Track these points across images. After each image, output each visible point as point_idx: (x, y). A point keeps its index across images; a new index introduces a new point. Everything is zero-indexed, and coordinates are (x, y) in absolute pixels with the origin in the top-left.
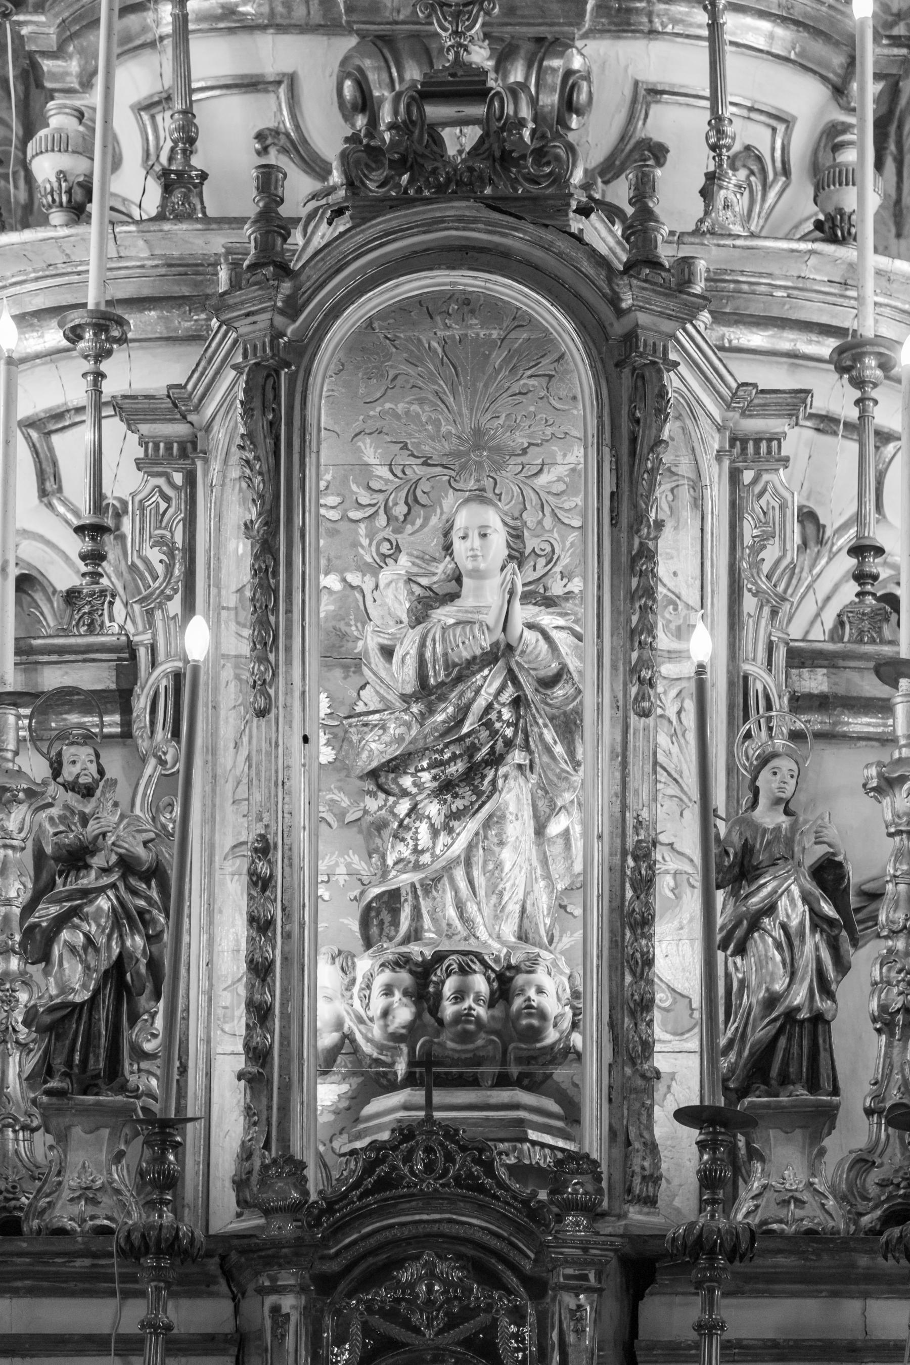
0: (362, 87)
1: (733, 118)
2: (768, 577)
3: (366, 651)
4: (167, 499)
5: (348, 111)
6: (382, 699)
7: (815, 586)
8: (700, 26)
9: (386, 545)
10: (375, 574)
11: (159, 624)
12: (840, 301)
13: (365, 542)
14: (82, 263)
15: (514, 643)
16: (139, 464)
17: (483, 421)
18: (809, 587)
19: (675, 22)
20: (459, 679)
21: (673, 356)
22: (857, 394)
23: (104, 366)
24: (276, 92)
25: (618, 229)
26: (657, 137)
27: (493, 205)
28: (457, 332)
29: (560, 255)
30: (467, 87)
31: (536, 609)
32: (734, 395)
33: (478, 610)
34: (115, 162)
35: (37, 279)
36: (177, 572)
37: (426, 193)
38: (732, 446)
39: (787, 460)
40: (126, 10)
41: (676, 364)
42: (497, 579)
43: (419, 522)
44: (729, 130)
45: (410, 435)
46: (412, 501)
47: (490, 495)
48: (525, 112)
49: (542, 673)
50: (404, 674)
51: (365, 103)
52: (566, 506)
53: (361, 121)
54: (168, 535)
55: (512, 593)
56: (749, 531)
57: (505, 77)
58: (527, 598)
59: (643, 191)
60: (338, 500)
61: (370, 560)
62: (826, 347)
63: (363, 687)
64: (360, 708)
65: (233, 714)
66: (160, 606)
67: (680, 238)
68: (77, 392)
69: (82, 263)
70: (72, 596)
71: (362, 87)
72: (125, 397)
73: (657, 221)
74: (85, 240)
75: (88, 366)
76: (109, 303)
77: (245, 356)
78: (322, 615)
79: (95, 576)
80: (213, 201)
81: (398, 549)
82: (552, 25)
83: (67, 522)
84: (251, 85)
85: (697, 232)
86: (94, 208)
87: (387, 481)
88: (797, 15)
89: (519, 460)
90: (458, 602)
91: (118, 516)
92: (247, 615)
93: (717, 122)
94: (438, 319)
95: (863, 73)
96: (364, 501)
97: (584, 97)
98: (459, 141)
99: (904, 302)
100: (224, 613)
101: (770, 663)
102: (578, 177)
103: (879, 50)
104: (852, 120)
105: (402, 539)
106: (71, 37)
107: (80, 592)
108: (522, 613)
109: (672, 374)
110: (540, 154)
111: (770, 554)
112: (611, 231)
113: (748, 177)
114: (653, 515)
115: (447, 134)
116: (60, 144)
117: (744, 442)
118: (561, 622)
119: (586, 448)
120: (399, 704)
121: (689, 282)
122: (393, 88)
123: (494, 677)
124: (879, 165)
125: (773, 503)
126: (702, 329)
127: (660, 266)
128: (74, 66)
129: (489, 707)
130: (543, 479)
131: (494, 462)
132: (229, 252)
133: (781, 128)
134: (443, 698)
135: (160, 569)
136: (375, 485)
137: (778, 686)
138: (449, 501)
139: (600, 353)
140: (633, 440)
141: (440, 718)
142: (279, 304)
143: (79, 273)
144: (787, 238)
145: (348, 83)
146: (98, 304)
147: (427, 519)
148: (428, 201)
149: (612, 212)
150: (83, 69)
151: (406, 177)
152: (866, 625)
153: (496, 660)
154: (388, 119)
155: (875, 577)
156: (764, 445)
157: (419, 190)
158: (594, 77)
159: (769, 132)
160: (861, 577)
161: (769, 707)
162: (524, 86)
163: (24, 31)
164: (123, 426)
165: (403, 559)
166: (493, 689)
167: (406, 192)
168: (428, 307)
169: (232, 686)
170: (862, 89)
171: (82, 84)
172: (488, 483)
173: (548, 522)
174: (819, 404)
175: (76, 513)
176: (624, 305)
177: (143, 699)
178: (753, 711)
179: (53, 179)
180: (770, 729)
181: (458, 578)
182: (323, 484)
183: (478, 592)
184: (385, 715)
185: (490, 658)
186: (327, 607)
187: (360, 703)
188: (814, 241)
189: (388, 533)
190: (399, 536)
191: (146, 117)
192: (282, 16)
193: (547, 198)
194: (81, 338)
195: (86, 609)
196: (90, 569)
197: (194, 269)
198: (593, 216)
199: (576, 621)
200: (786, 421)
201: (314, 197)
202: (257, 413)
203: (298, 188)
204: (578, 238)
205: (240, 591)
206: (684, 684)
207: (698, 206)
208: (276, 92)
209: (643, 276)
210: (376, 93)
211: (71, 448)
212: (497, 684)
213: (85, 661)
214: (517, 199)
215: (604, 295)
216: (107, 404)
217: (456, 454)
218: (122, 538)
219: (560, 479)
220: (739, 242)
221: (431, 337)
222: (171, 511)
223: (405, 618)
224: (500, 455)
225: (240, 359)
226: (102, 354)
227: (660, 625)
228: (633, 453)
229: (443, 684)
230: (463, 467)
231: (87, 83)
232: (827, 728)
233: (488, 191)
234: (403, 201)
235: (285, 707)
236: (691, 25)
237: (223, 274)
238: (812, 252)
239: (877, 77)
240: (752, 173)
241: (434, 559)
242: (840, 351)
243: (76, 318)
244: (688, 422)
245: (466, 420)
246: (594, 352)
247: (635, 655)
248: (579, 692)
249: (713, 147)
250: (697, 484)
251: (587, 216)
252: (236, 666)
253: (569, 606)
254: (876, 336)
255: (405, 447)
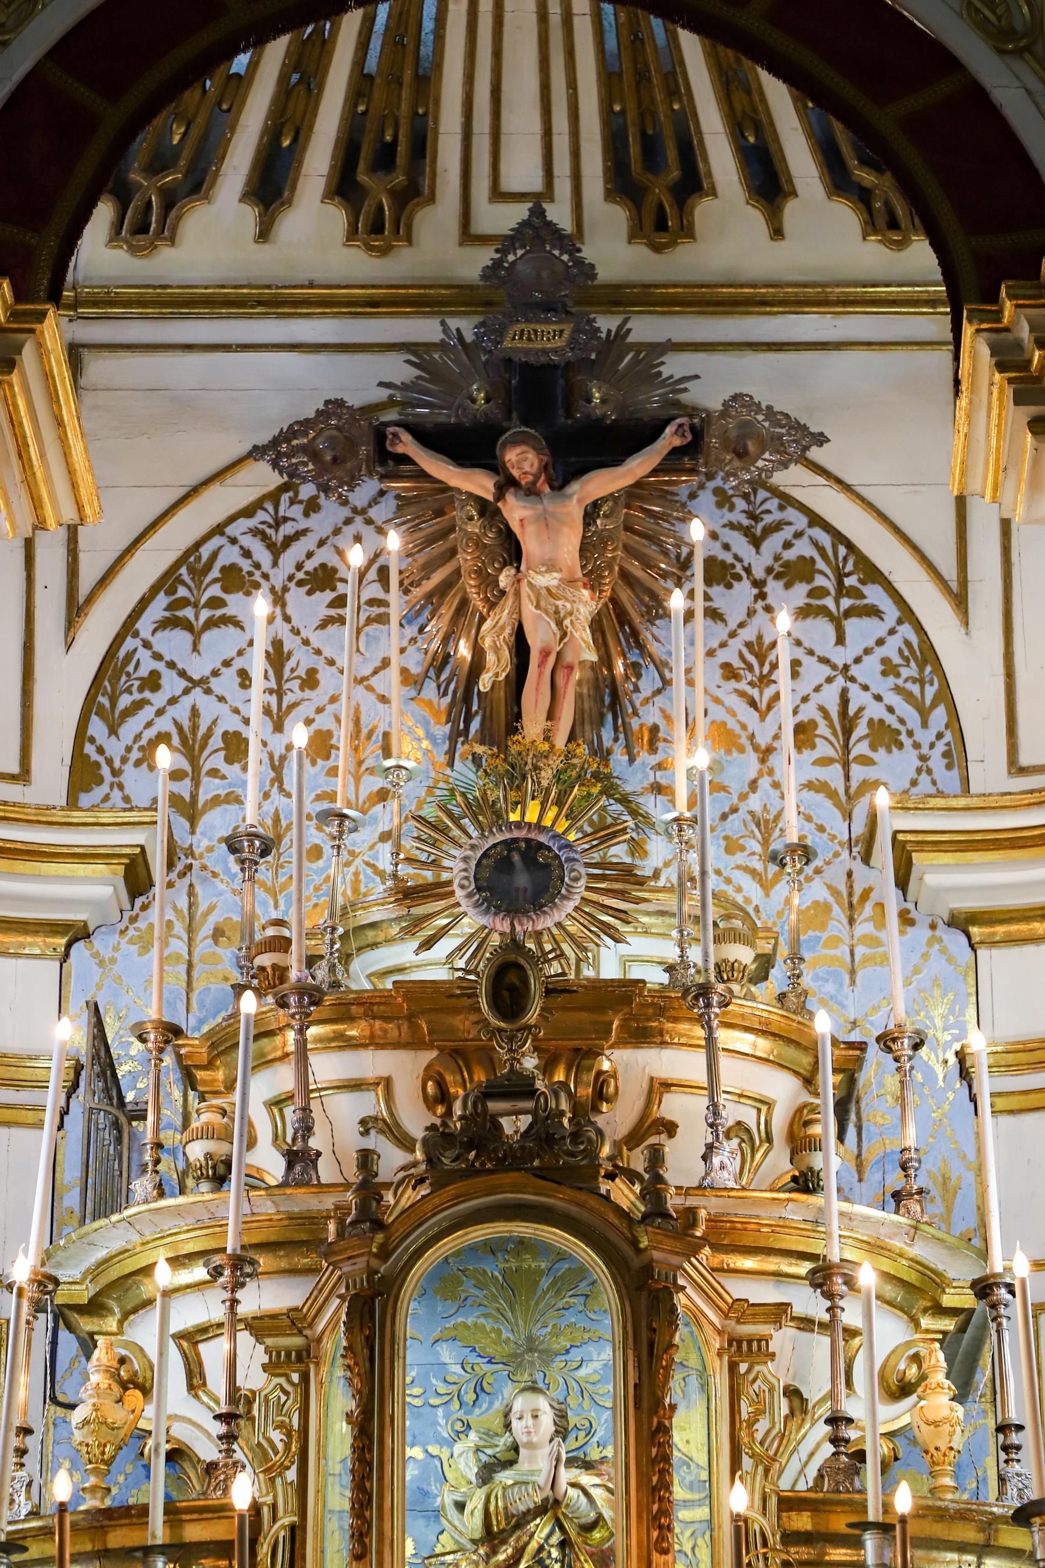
0: (441, 1085)
1: (726, 1103)
2: (762, 1443)
3: (443, 1506)
4: (286, 1393)
5: (430, 1103)
6: (456, 1542)
7: (800, 1448)
8: (699, 1038)
9: (460, 1424)
10: (451, 1446)
11: (279, 1489)
12: (813, 1234)
13: (442, 1422)
14: (223, 1218)
15: (560, 1499)
16: (265, 1368)
17: (534, 1331)
18: (795, 1449)
19: (681, 1036)
20: (518, 1526)
21: (681, 1282)
22: (828, 1304)
23: (239, 1295)
24: (375, 1090)
25: (637, 1188)
26: (669, 1116)
27: (540, 1174)
28: (513, 1264)
29: (591, 1210)
30: (519, 1088)
31: (578, 1471)
32: (730, 1308)
33: (532, 1472)
34: (251, 1143)
35: (188, 1231)
36: (294, 1449)
37: (489, 1166)
38: (730, 1345)
39: (773, 1355)
40: (257, 1037)
41: (683, 1288)
42: (547, 1449)
43: (485, 1406)
44: (724, 1113)
45: (478, 1341)
46: (480, 1389)
47: (541, 1385)
48: (564, 1105)
49: (583, 1521)
50: (473, 1523)
51: (444, 1097)
52: (601, 1392)
53: (440, 1110)
54: (287, 1420)
55: (558, 1460)
56: (745, 1409)
57: (551, 1077)
58: (571, 1462)
59: (656, 1158)
60: (421, 1391)
61: (446, 1435)
62: (804, 1268)
63: (442, 1532)
64: (439, 1549)
65: (336, 1556)
66: (280, 1474)
67: (687, 1192)
68: (218, 1313)
69: (223, 1218)
70: (211, 1468)
71: (441, 1085)
72: (254, 1318)
73: (666, 1184)
74: (226, 1202)
75: (227, 1295)
76: (243, 1247)
77: (347, 1288)
78: (408, 1478)
79: (229, 1452)
80: (326, 1171)
81: (469, 1427)
82: (587, 1039)
83: (209, 1408)
84: (355, 1086)
85: (700, 1187)
86: (233, 1176)
87: (459, 1376)
88: (773, 1029)
89: (564, 1358)
90: (516, 1467)
91: (249, 1402)
92: (347, 1479)
93: (714, 1108)
94: (499, 1255)
95: (825, 1071)
96: (441, 1391)
97: (612, 1089)
98: (514, 1125)
99: (863, 1234)
100: (330, 1479)
101: (764, 1508)
102: (606, 1151)
103: (837, 1052)
104: (817, 1101)
105: (472, 1419)
106: (218, 1055)
107: (217, 1464)
108: (566, 1475)
109: (681, 1295)
110: (576, 1136)
111: (762, 1426)
112: (631, 1190)
113: (740, 1145)
114: (667, 1401)
115: (504, 1121)
116: (208, 1133)
117: (739, 1342)
118: (597, 1480)
119: (614, 1351)
120: (469, 1546)
121: (694, 1224)
122: (465, 1089)
123: (544, 1526)
124: (841, 1137)
125: (763, 1387)
126: (704, 1263)
127: (670, 1216)
128: (220, 1075)
129: (541, 1548)
130: (582, 1372)
131: (543, 1361)
132: (337, 1208)
133: (764, 1109)
134: (504, 1542)
135: (280, 1446)
136: (449, 1379)
137: (772, 1527)
138: (509, 1390)
139: (623, 1280)
140: (651, 1345)
141: (501, 1557)
142: (374, 1250)
143: (221, 1226)
144: (771, 1191)
145: (430, 1083)
146: (234, 1250)
147: (491, 1404)
148: (490, 1172)
149: (632, 1176)
150: (226, 1077)
151: (473, 1153)
152: (841, 1478)
153: (545, 1513)
154: (459, 1113)
155: (847, 1441)
156: (755, 1344)
157: (483, 1164)
158: (620, 1076)
159: (755, 1111)
160: (835, 1440)
161: (765, 1544)
162: (564, 1085)
163: (183, 1051)
164: (253, 1340)
165: (473, 1436)
166: (544, 1535)
167: (473, 1165)
168: (491, 1248)
169: (337, 1534)
170: (825, 1083)
171: (226, 1087)
172: (539, 1376)
173: (587, 1404)
174: (798, 1310)
175: (217, 1402)
176: (642, 1246)
177: (265, 1547)
178: (752, 1547)
179: (202, 1159)
180: (766, 1559)
181: (515, 1448)
182: (408, 1380)
183: (531, 1460)
184: (459, 1555)
185: (541, 1510)
186: (411, 1472)
187: (439, 1546)
188: (790, 1191)
189: (461, 1414)
190: (469, 1417)
191: (276, 1111)
192: (380, 1038)
193: (583, 1166)
194: (221, 1274)
195: (222, 1477)
196: (225, 1447)
197: (313, 1221)
198: (617, 1180)
199: (610, 1480)
200: (772, 1326)
201: (403, 1168)
202: (357, 1330)
203: (392, 1160)
204: (607, 1198)
205: (343, 1461)
206: (696, 1526)
207: (700, 1167)
208: (375, 1090)
209: (656, 1224)
210: (452, 1090)
211: (213, 1354)
212: (547, 1530)
213: (219, 1518)
214: (559, 1168)
215: (627, 1238)
216: (240, 1320)
217: (515, 1356)
218: (253, 1419)
219: (595, 1371)
220: (732, 1194)
221: (493, 1268)
222: (290, 1402)
223: (474, 1479)
224: (548, 1356)
225: (343, 1291)
226: (237, 1285)
227: (676, 1481)
228: (651, 1353)
229: (504, 1530)
230: (519, 1365)
231: (230, 1087)
232: (812, 1557)
233: (536, 1163)
234: (472, 1172)
235: (377, 1552)
236: (693, 1037)
237: (332, 1227)
238: (789, 1200)
239: (835, 1071)
240: (743, 1141)
241: (497, 1435)
242: (813, 1272)
243: (217, 1260)
244: (695, 1329)
245: (522, 1329)
246: (620, 1280)
247: (655, 1507)
248: (612, 1535)
249: (711, 1126)
250: (703, 1373)
251: (613, 1180)
252: (340, 1519)
253: (604, 1467)
254: (842, 1260)
255: (474, 1350)
